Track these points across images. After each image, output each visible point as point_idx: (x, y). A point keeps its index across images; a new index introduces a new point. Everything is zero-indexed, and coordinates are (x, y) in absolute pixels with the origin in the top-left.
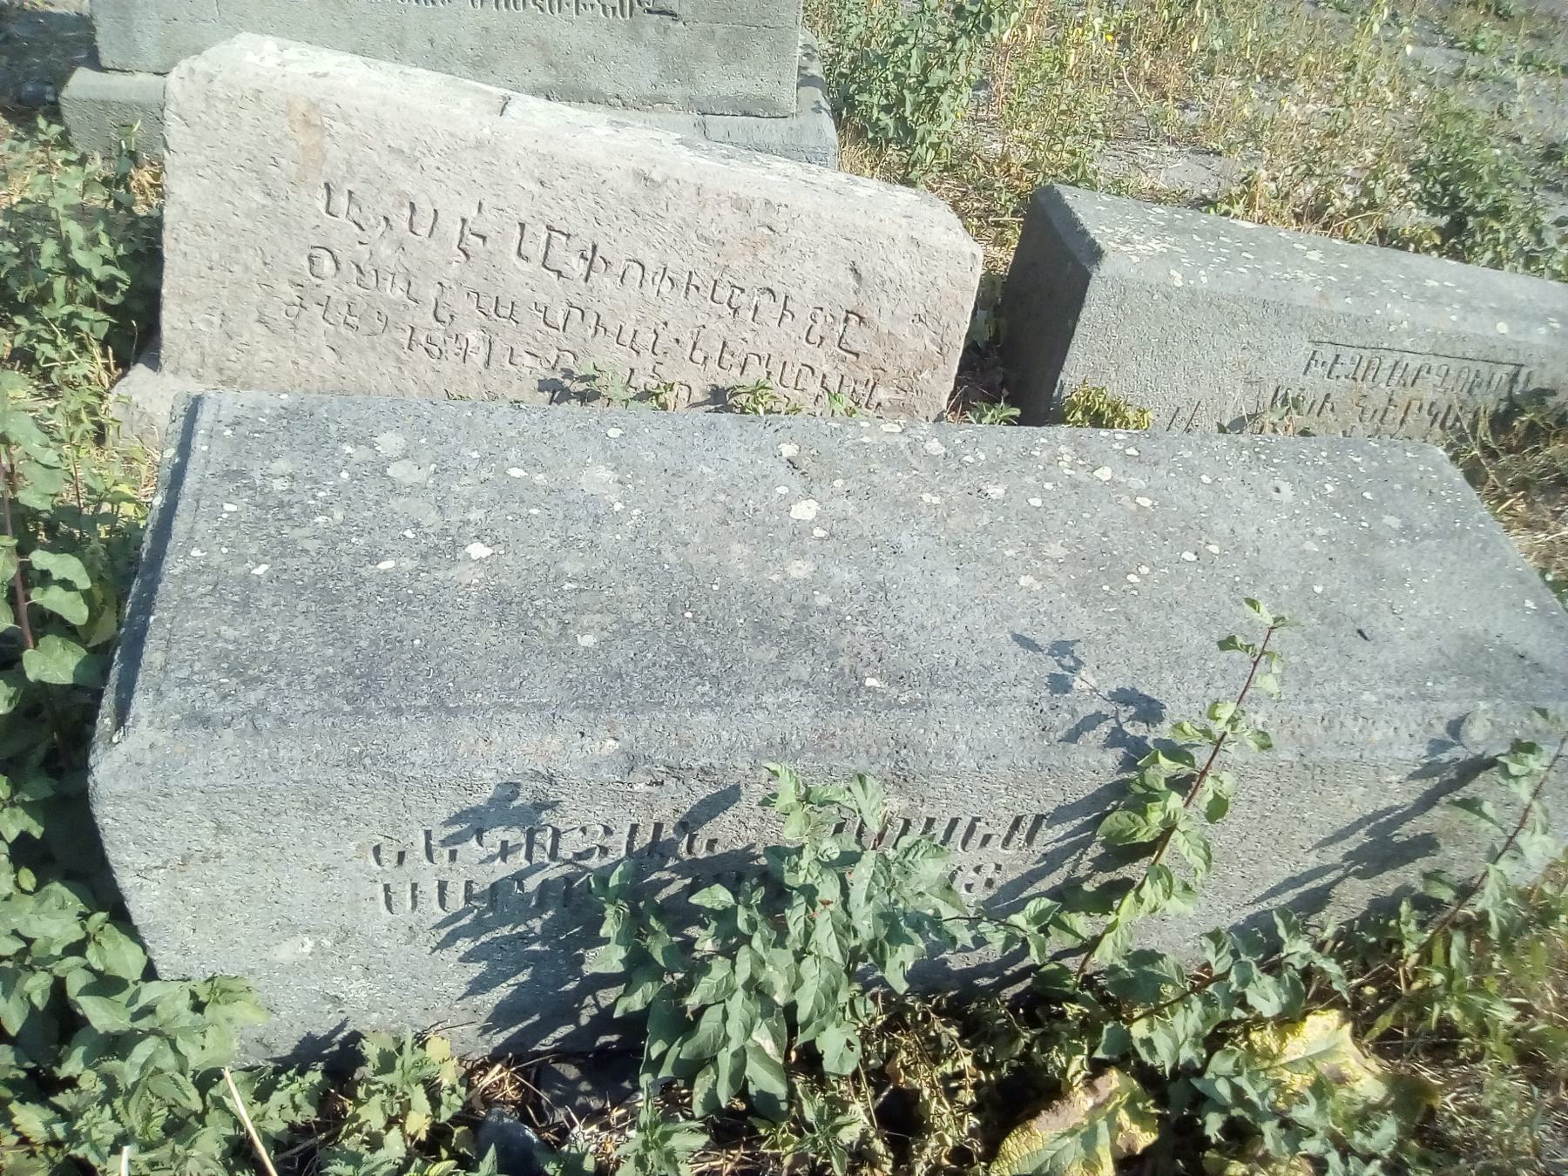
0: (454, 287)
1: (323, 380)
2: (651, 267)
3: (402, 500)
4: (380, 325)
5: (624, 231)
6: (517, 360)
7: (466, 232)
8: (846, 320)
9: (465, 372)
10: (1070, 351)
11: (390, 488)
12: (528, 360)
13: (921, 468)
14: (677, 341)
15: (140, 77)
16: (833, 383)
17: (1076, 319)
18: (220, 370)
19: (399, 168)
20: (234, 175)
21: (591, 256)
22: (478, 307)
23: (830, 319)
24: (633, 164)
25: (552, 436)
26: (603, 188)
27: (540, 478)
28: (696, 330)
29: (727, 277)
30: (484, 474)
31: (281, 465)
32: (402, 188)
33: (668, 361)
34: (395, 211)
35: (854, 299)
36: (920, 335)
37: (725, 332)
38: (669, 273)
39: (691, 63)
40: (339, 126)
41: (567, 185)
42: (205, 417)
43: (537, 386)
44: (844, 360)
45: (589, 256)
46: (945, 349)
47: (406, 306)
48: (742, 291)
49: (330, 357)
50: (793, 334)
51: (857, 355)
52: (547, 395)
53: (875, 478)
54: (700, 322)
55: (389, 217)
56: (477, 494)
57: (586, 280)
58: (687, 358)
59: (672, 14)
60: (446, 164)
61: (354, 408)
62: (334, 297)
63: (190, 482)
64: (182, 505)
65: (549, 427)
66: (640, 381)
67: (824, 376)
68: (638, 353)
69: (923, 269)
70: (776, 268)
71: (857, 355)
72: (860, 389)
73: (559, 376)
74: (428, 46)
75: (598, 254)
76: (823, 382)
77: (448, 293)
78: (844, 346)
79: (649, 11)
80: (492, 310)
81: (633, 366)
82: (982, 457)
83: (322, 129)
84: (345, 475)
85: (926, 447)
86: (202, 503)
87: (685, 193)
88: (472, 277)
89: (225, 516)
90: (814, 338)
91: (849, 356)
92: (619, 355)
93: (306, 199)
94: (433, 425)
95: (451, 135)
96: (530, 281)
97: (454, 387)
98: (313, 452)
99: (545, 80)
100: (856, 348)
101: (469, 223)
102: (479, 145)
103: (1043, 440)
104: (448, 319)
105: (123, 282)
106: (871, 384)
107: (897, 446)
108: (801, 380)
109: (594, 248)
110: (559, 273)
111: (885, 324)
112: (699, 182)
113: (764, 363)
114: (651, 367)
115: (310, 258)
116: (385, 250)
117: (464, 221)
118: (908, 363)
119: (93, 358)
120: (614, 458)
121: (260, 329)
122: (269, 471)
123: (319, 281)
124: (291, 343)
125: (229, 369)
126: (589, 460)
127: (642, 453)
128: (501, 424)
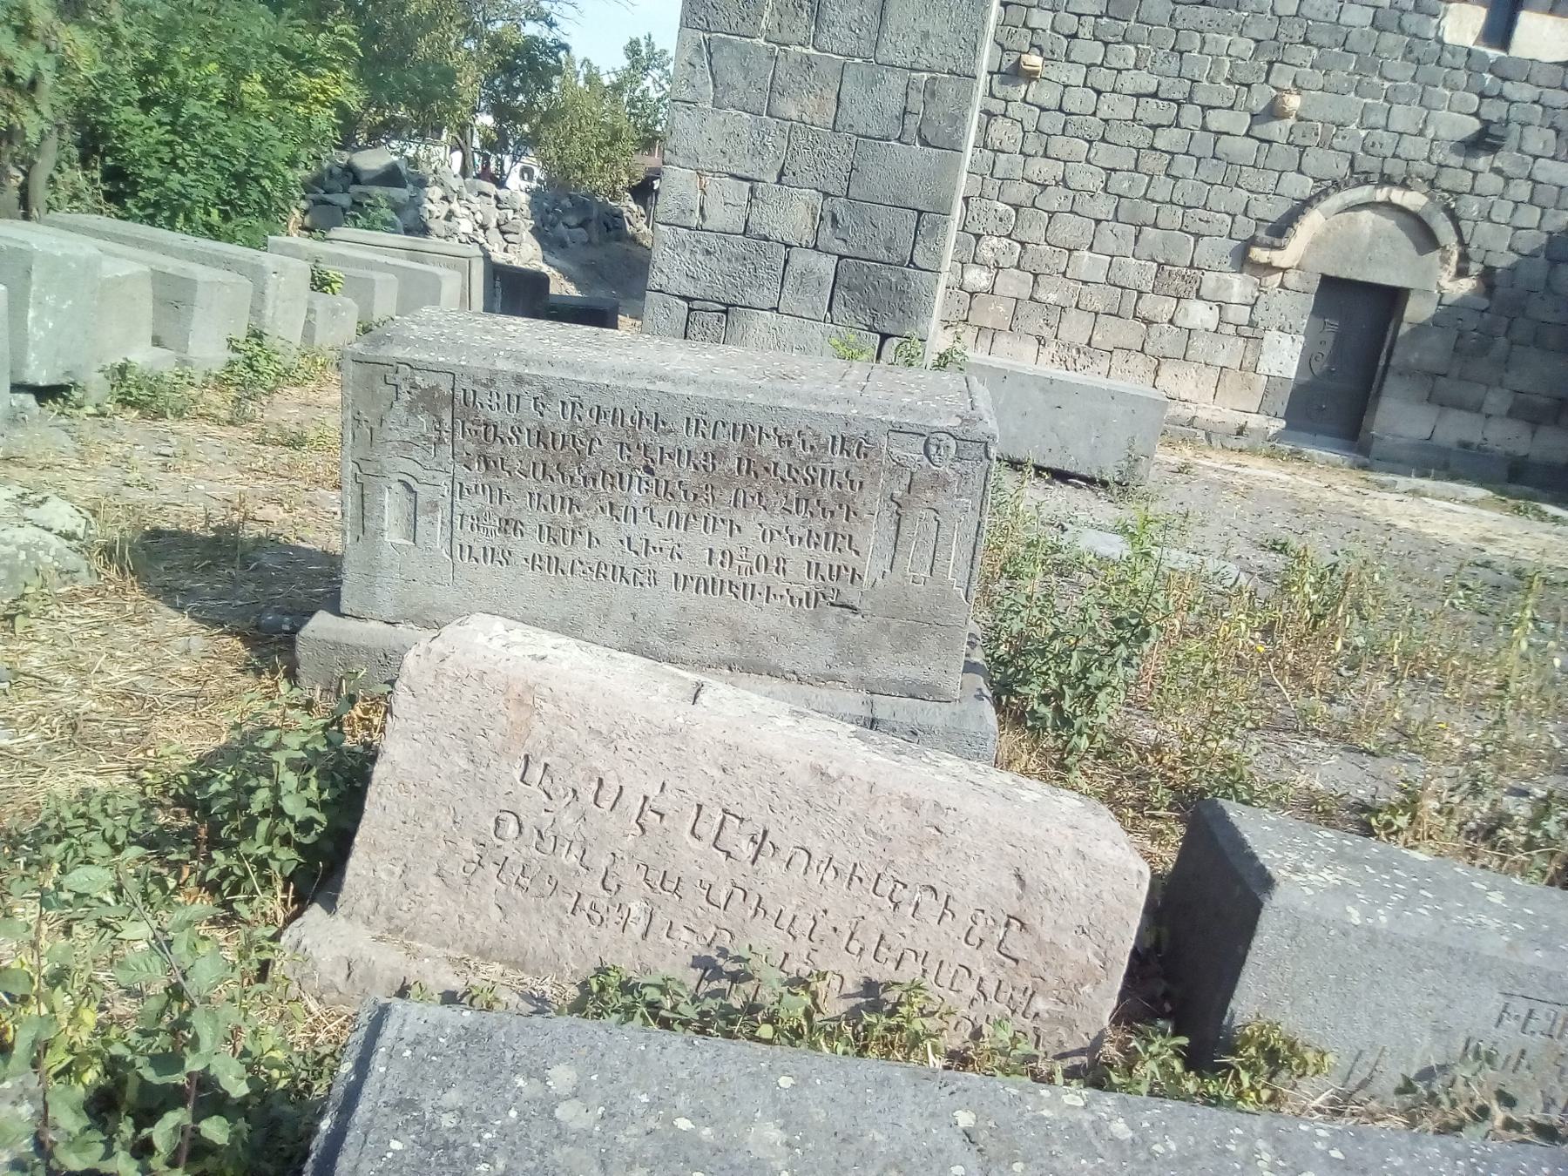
0: (626, 858)
1: (485, 937)
2: (818, 855)
3: (566, 1149)
4: (549, 888)
5: (795, 820)
6: (675, 934)
7: (646, 808)
8: (1007, 925)
9: (622, 940)
10: (1241, 979)
11: (555, 1132)
12: (686, 935)
13: (1107, 1155)
14: (835, 929)
15: (372, 624)
16: (990, 987)
17: (1247, 946)
18: (390, 919)
19: (595, 747)
20: (444, 741)
21: (760, 841)
22: (645, 879)
23: (990, 922)
24: (811, 759)
25: (723, 1081)
26: (781, 780)
27: (706, 1132)
28: (854, 921)
29: (890, 872)
30: (651, 1123)
31: (453, 1097)
32: (594, 764)
33: (823, 949)
34: (584, 785)
35: (1016, 904)
36: (1082, 946)
37: (884, 926)
38: (834, 863)
39: (866, 649)
40: (548, 707)
41: (748, 773)
42: (389, 1032)
43: (690, 960)
44: (1002, 965)
45: (759, 841)
46: (1109, 965)
47: (577, 872)
48: (905, 886)
49: (496, 914)
50: (952, 934)
51: (1017, 961)
52: (699, 971)
53: (1057, 1165)
54: (859, 913)
55: (577, 789)
56: (641, 1149)
57: (753, 862)
58: (843, 947)
59: (854, 609)
60: (638, 746)
61: (531, 1033)
62: (511, 859)
63: (363, 1109)
64: (349, 1139)
65: (720, 1070)
66: (793, 966)
67: (981, 979)
68: (794, 938)
69: (1088, 881)
70: (940, 867)
71: (1017, 961)
72: (1018, 996)
73: (713, 954)
74: (631, 619)
75: (768, 839)
76: (979, 985)
77: (619, 863)
78: (1003, 951)
79: (832, 604)
80: (658, 883)
81: (788, 951)
82: (1173, 1147)
83: (533, 708)
84: (513, 1114)
85: (1111, 1128)
86: (371, 1137)
87: (857, 789)
88: (645, 850)
89: (389, 1155)
90: (974, 939)
91: (1008, 961)
92: (775, 938)
93: (506, 769)
94: (606, 1059)
95: (648, 721)
96: (700, 860)
97: (609, 955)
98: (486, 1083)
99: (728, 652)
100: (1017, 954)
101: (650, 801)
102: (671, 732)
103: (1238, 1131)
104: (614, 888)
105: (321, 824)
106: (1029, 992)
107: (1079, 1125)
108: (957, 981)
109: (765, 833)
110: (728, 854)
111: (1047, 933)
112: (872, 781)
113: (920, 960)
114: (806, 953)
115: (497, 820)
116: (567, 819)
117: (646, 798)
118: (1069, 974)
119: (275, 894)
120: (785, 1114)
121: (435, 882)
122: (440, 1103)
123: (500, 842)
124: (462, 898)
125: (398, 918)
126: (758, 1114)
127: (813, 1109)
128: (672, 1063)
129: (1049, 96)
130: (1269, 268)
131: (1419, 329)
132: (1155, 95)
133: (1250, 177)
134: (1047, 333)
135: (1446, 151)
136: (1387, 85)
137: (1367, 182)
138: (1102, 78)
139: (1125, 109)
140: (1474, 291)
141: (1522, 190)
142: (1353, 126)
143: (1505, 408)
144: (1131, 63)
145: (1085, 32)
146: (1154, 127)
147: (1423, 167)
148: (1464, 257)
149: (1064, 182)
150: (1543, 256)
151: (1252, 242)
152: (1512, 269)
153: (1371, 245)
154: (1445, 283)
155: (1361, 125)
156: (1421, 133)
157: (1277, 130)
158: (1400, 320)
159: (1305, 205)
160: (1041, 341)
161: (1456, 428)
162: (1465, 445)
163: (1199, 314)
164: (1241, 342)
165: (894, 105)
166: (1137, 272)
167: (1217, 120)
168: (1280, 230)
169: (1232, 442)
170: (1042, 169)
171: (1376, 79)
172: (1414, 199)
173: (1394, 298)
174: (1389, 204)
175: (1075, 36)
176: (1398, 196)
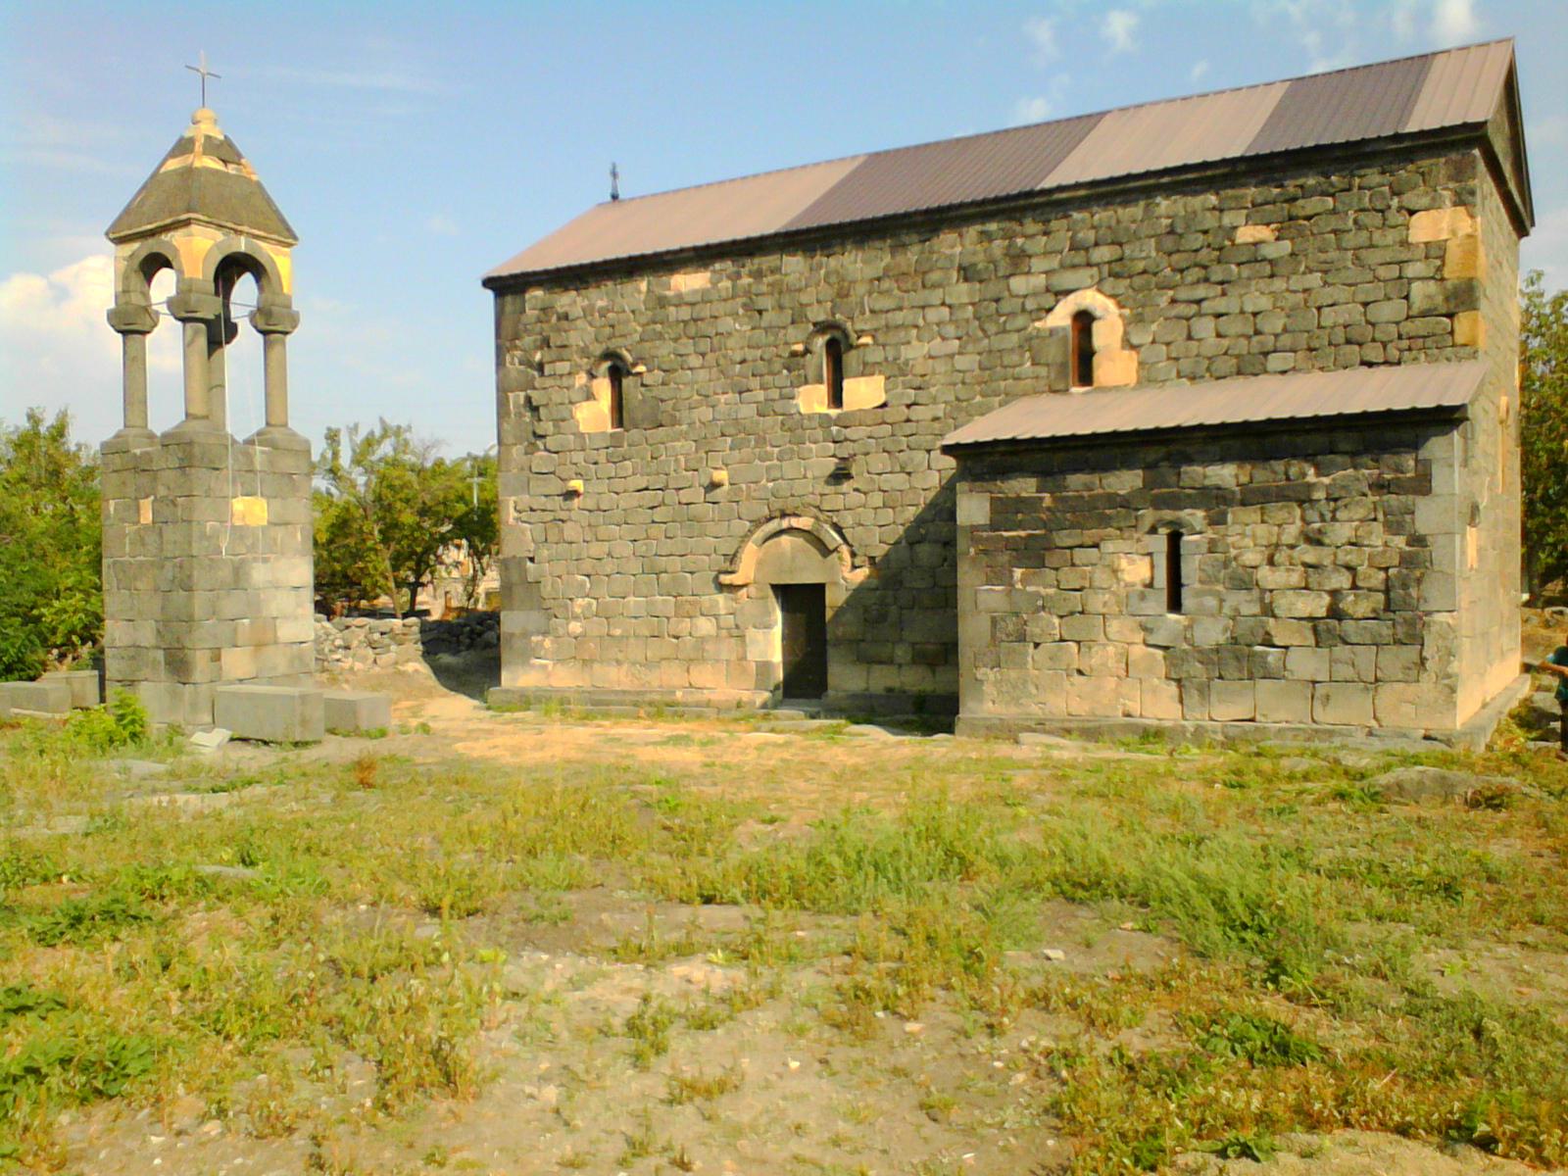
129: (590, 504)
130: (733, 588)
131: (840, 612)
132: (647, 489)
133: (711, 528)
134: (620, 656)
135: (822, 481)
136: (776, 450)
137: (770, 519)
138: (618, 484)
139: (628, 501)
140: (869, 577)
141: (877, 499)
142: (764, 481)
143: (909, 658)
144: (630, 472)
145: (602, 459)
146: (652, 508)
147: (810, 499)
148: (853, 555)
149: (609, 554)
150: (904, 542)
151: (721, 572)
152: (886, 555)
153: (793, 559)
154: (847, 575)
155: (768, 481)
156: (805, 477)
157: (718, 494)
158: (824, 606)
159: (745, 537)
160: (619, 663)
161: (881, 679)
162: (890, 690)
163: (705, 626)
164: (733, 640)
165: (170, 576)
166: (664, 603)
167: (684, 496)
168: (733, 558)
169: (737, 714)
170: (597, 549)
171: (769, 448)
172: (804, 522)
173: (815, 593)
174: (790, 530)
175: (596, 463)
176: (795, 522)
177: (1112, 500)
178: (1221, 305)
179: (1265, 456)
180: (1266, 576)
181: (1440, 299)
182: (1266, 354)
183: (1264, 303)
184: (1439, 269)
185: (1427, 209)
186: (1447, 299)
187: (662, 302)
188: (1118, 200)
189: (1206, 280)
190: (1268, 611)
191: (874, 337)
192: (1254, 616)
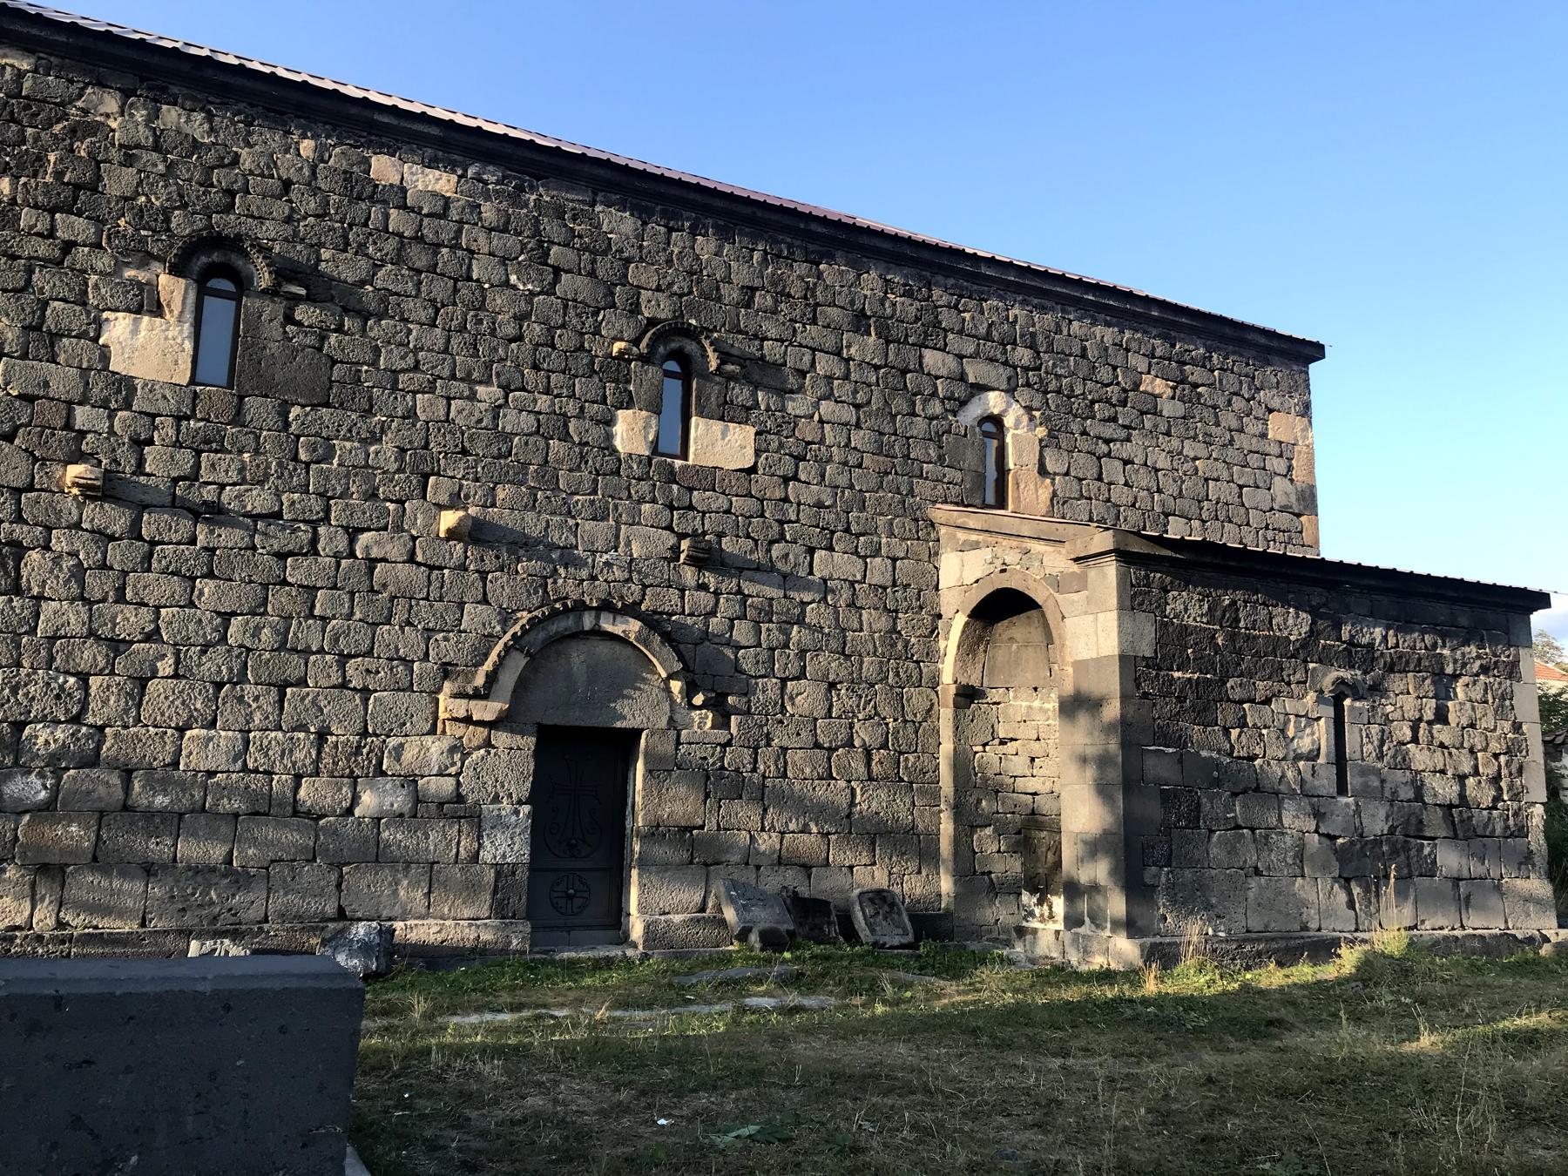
133: (425, 614)
146: (282, 556)
175: (150, 442)
177: (1277, 645)
178: (1126, 450)
179: (1403, 623)
180: (1420, 758)
181: (1293, 498)
182: (1167, 515)
183: (1163, 462)
184: (1290, 468)
185: (1279, 411)
186: (1298, 500)
187: (359, 188)
188: (1036, 301)
189: (1114, 419)
190: (1419, 796)
191: (743, 367)
192: (1409, 801)
